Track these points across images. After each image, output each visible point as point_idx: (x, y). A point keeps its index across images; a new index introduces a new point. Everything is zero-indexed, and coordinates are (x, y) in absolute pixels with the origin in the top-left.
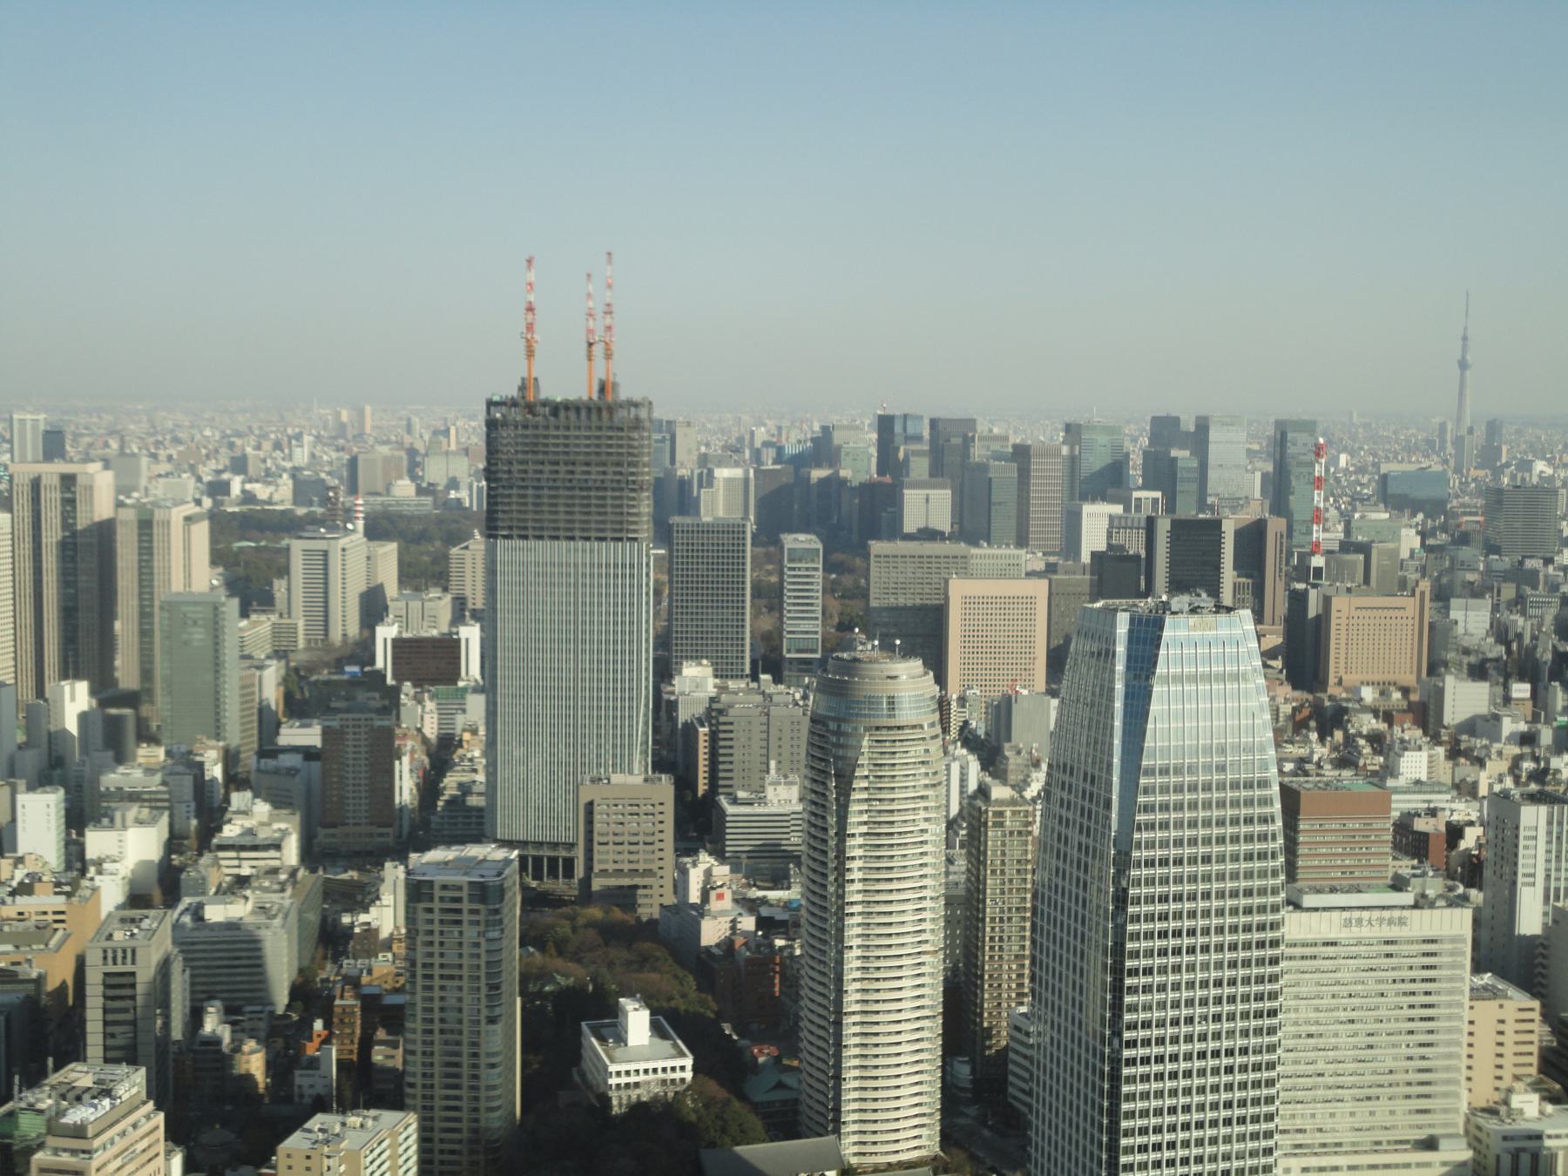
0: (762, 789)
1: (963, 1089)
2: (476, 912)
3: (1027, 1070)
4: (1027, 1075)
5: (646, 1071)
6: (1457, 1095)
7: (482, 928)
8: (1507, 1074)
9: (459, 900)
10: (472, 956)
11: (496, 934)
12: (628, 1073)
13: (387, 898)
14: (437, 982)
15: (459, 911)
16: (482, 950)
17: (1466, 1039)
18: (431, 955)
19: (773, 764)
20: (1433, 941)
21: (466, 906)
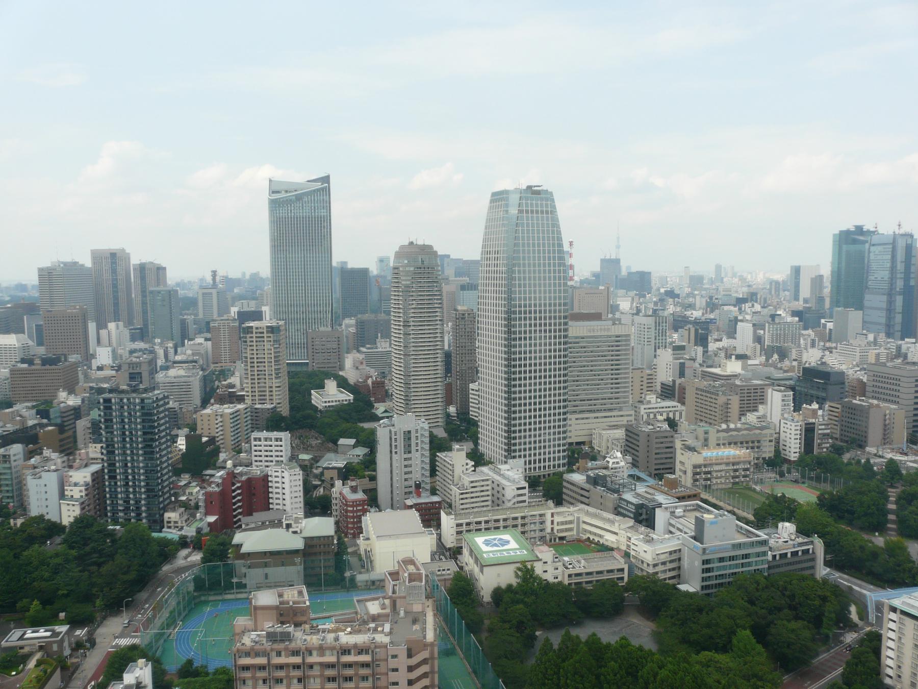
0: (376, 344)
1: (454, 416)
2: (270, 337)
3: (477, 412)
4: (477, 415)
5: (336, 401)
6: (628, 398)
7: (272, 343)
8: (644, 387)
9: (263, 333)
10: (268, 354)
11: (277, 346)
12: (329, 402)
13: (237, 374)
14: (256, 365)
15: (263, 337)
16: (272, 352)
17: (631, 392)
18: (253, 354)
19: (379, 335)
20: (619, 337)
21: (265, 335)
